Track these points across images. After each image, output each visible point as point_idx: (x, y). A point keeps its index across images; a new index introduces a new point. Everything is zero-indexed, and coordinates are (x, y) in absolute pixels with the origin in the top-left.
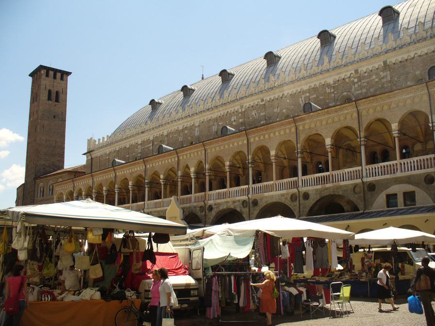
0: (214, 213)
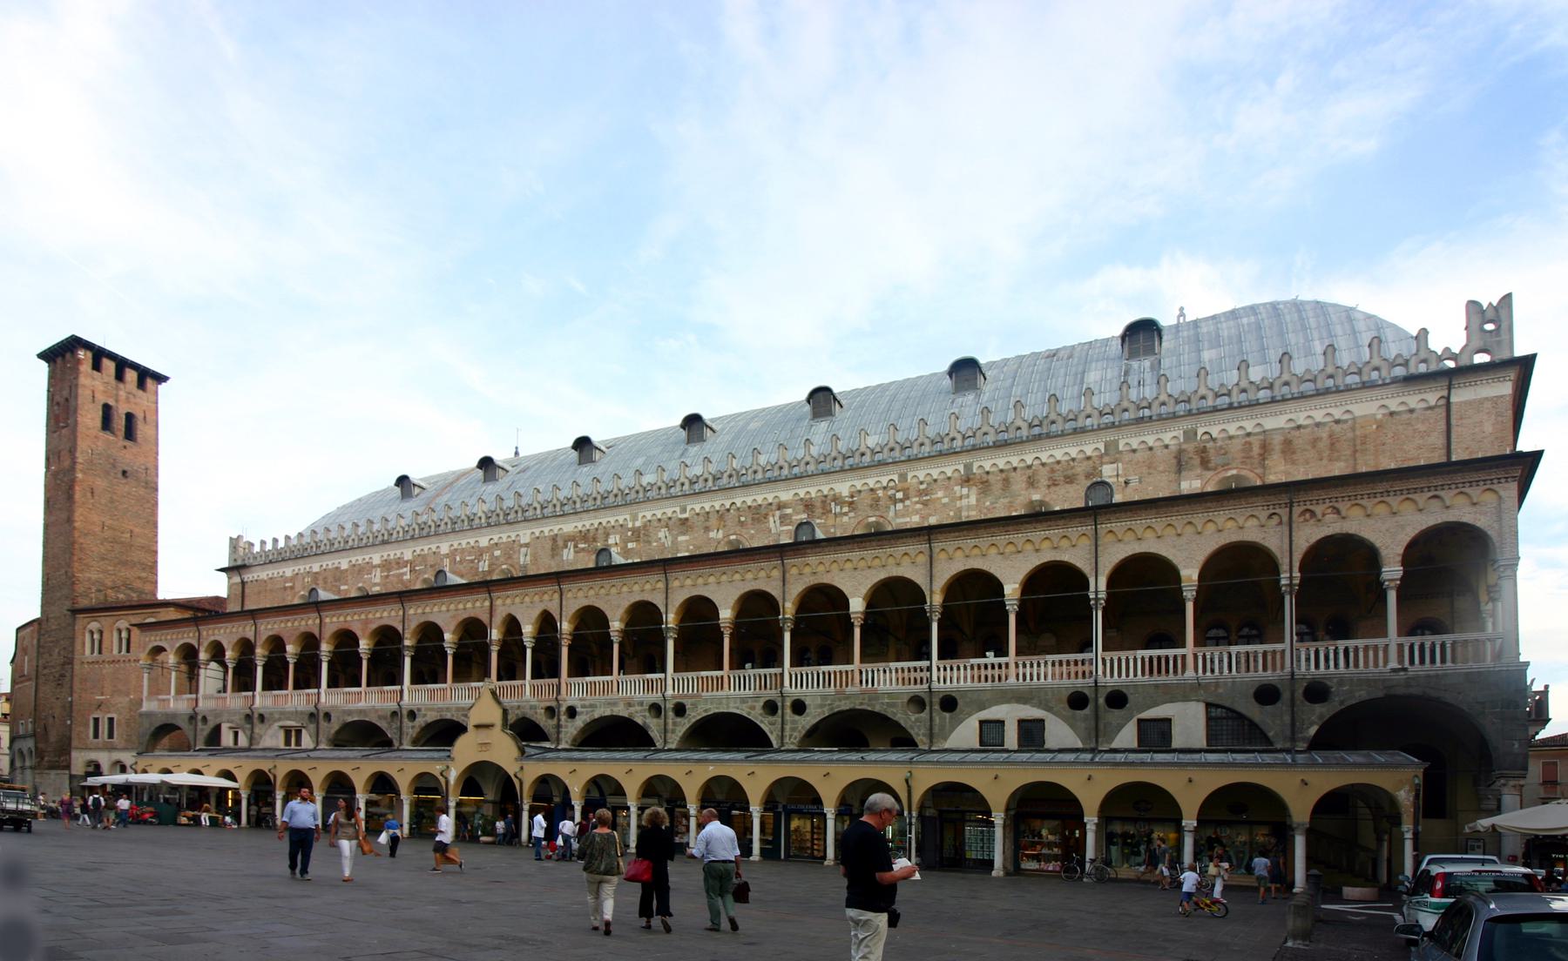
0: (580, 722)
